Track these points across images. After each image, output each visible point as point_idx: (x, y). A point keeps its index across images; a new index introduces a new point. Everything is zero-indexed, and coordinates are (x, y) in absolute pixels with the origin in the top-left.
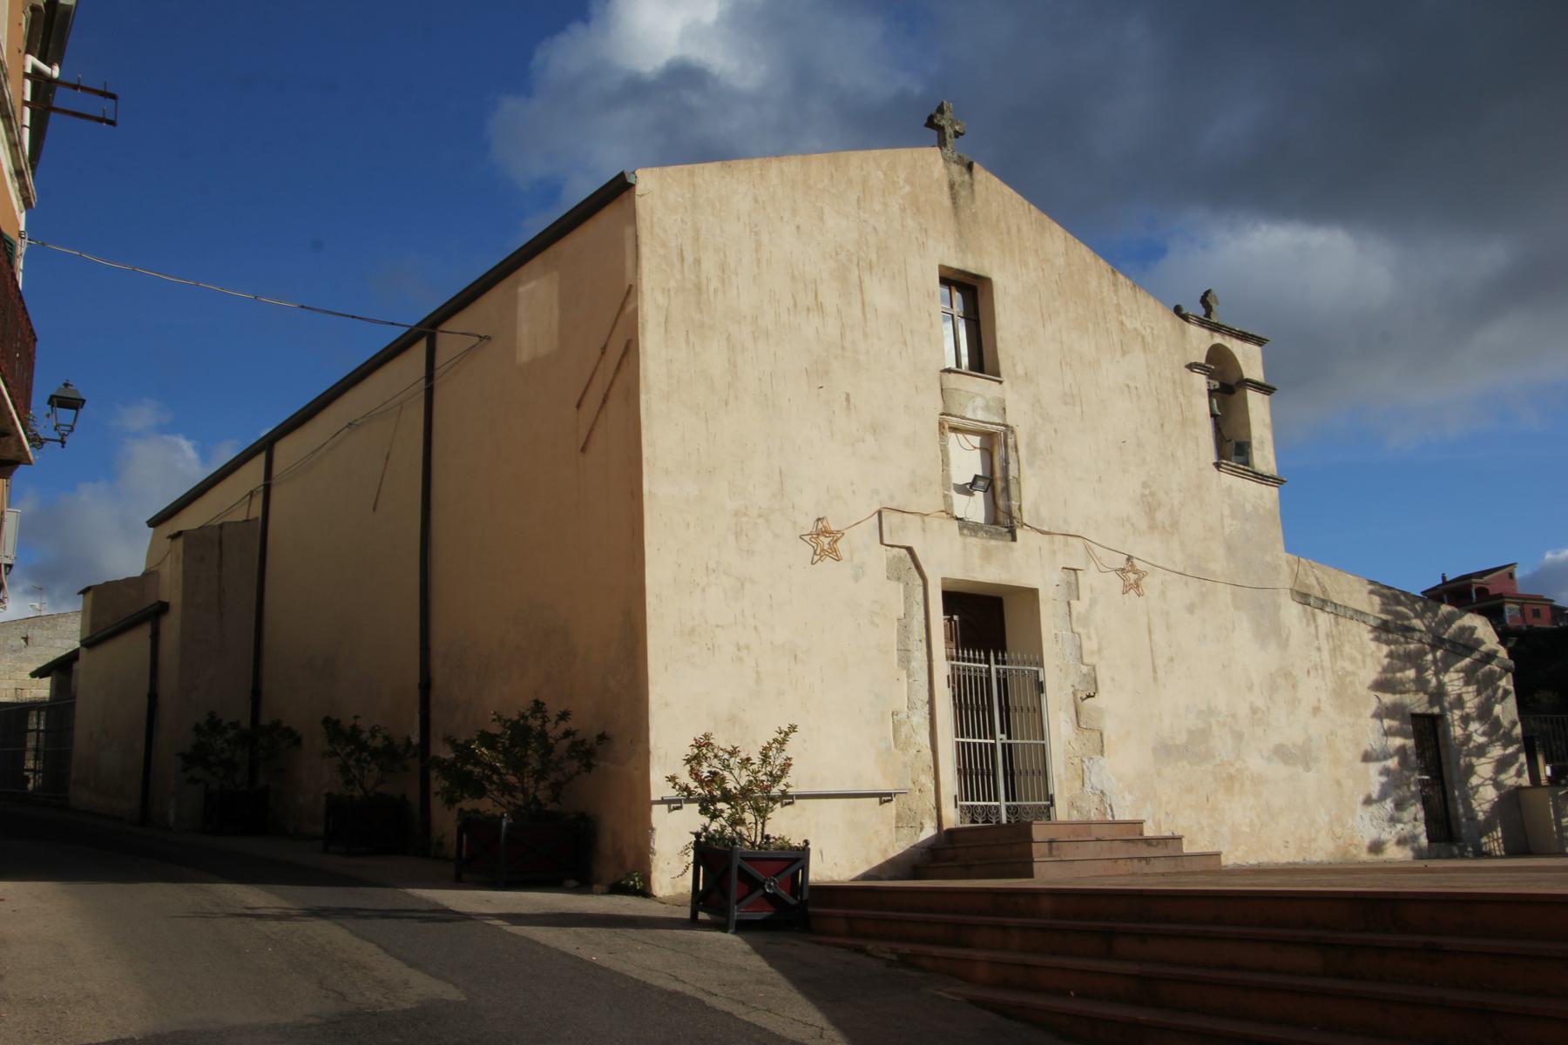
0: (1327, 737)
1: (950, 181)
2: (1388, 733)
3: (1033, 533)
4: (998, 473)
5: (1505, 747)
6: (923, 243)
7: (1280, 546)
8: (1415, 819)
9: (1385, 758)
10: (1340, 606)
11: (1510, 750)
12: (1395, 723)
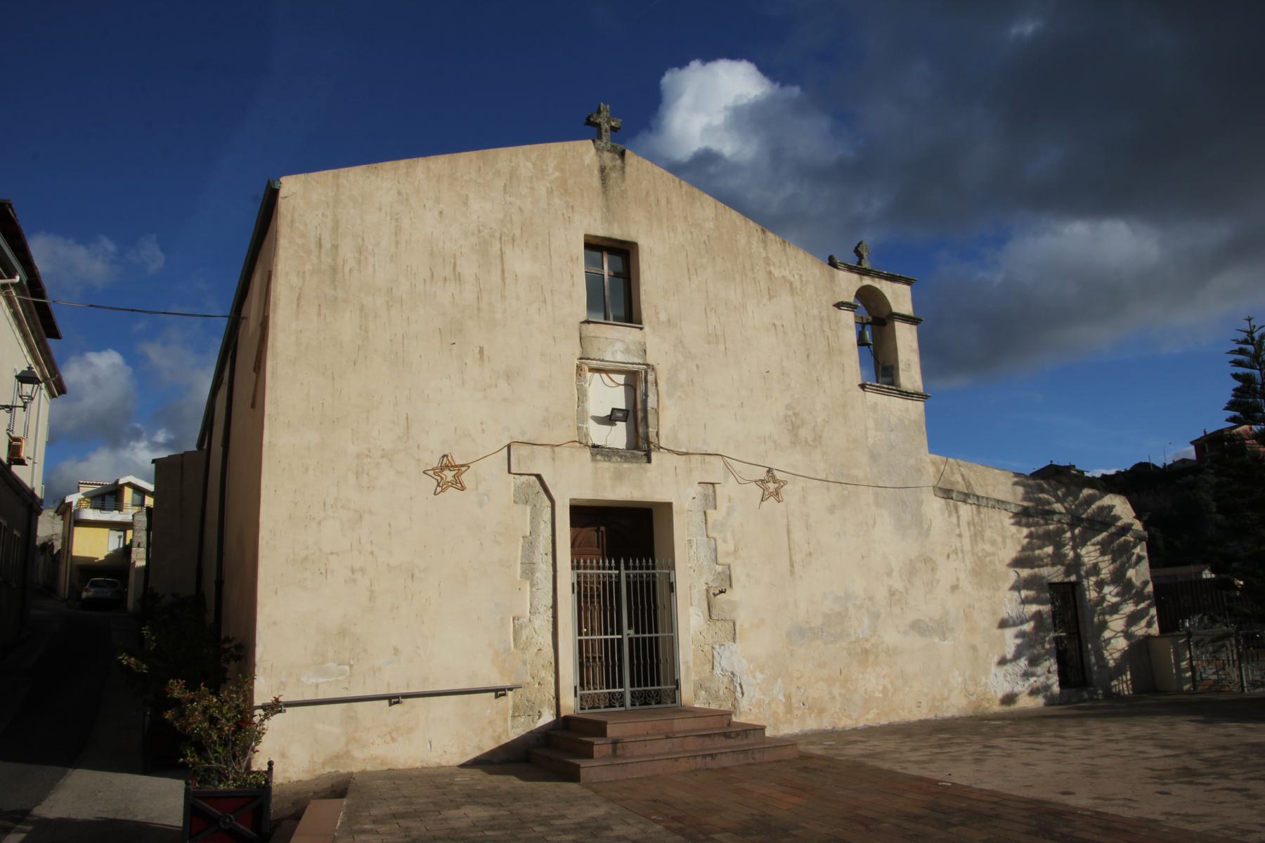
0: (964, 610)
1: (601, 166)
2: (1025, 602)
3: (669, 456)
4: (639, 406)
5: (1137, 604)
6: (569, 217)
7: (925, 450)
8: (1049, 672)
9: (1022, 623)
10: (983, 497)
11: (1142, 605)
12: (1031, 593)
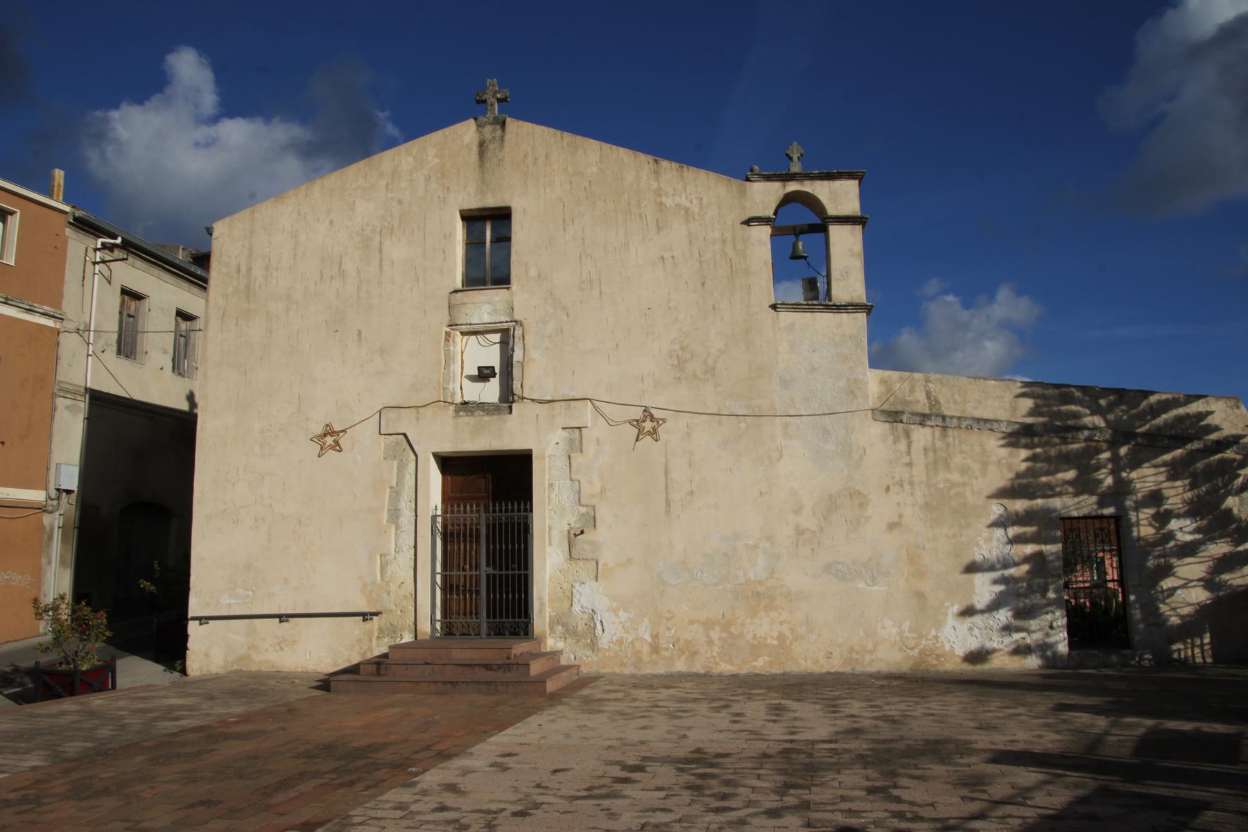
2: (1014, 541)
